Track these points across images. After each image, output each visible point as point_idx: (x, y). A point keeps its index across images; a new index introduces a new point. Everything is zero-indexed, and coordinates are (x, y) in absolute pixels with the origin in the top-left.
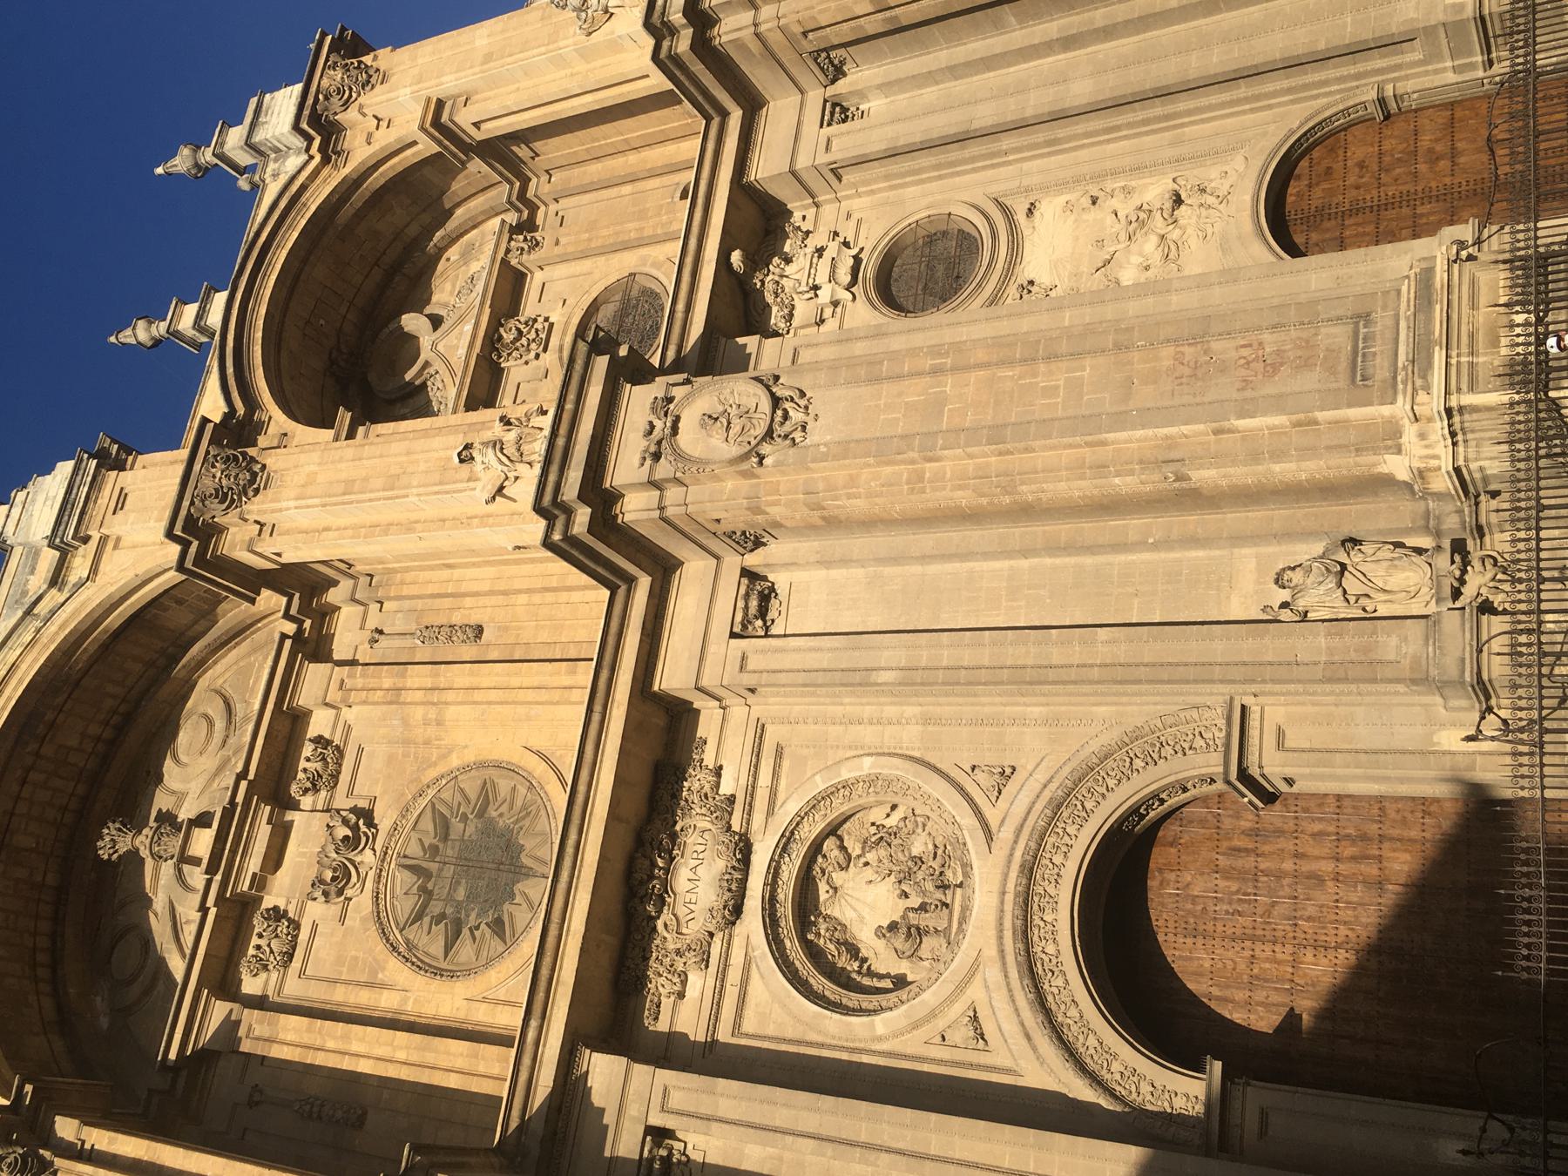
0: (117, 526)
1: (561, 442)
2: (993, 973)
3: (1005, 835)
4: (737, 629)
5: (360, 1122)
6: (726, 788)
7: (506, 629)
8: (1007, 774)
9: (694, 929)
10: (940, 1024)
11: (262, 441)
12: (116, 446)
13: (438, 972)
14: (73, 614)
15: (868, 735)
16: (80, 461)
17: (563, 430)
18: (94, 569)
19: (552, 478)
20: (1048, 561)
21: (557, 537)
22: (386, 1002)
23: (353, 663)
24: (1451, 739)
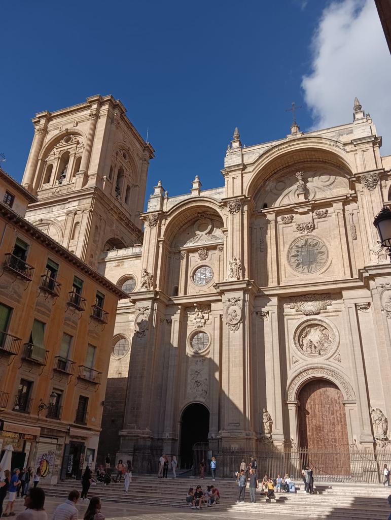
0: (359, 152)
1: (381, 267)
2: (304, 364)
3: (328, 362)
4: (357, 304)
5: (261, 252)
6: (328, 307)
7: (357, 245)
8: (339, 361)
9: (302, 308)
10: (295, 355)
11: (383, 182)
12: (379, 141)
13: (288, 256)
14: (338, 152)
15: (342, 333)
16: (373, 136)
17: (383, 267)
18: (349, 152)
19: (372, 268)
20: (379, 365)
21: (361, 271)
22: (282, 248)
23: (344, 211)
24: (355, 437)
